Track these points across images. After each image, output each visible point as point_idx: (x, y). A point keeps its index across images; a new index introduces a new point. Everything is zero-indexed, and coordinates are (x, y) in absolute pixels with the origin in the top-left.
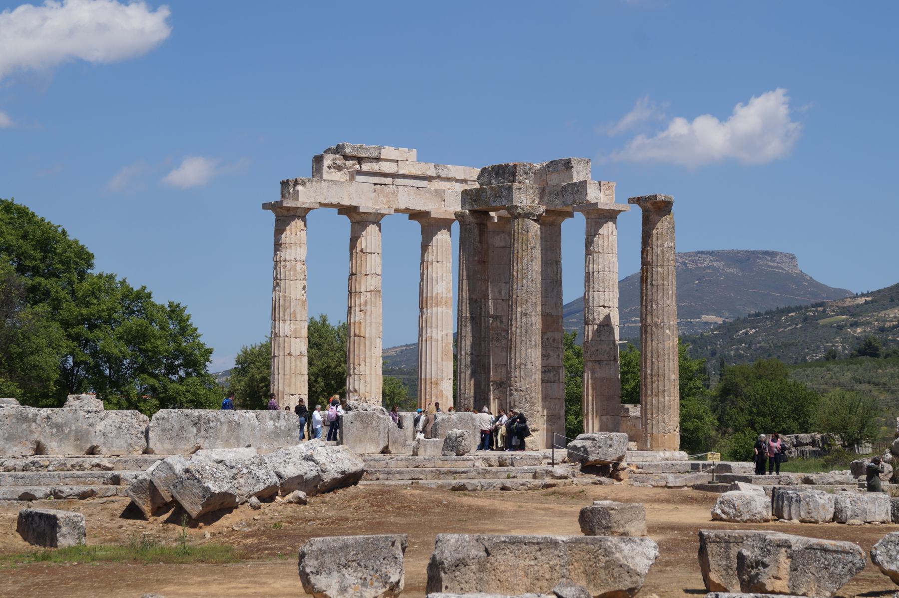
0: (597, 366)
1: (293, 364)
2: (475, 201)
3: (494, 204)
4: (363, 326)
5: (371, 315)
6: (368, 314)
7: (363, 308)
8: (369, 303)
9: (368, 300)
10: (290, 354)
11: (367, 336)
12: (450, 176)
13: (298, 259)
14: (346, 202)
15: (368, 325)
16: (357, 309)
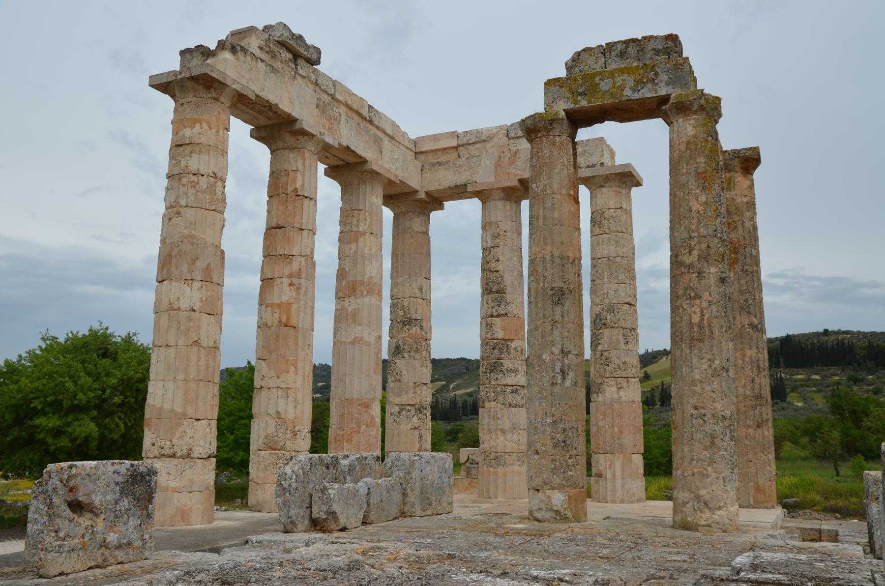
0: (623, 382)
1: (202, 362)
2: (583, 94)
3: (636, 96)
4: (294, 308)
5: (305, 293)
6: (302, 290)
7: (295, 281)
8: (304, 275)
9: (303, 269)
10: (196, 343)
11: (300, 326)
12: (381, 125)
13: (219, 175)
14: (285, 107)
15: (302, 308)
16: (286, 281)
